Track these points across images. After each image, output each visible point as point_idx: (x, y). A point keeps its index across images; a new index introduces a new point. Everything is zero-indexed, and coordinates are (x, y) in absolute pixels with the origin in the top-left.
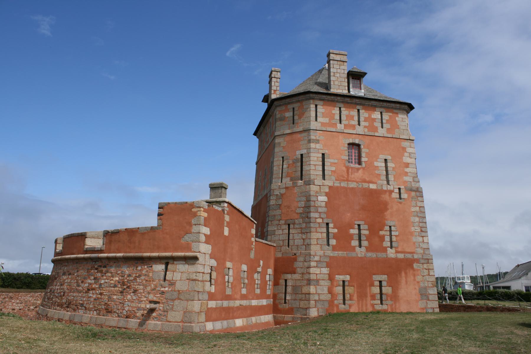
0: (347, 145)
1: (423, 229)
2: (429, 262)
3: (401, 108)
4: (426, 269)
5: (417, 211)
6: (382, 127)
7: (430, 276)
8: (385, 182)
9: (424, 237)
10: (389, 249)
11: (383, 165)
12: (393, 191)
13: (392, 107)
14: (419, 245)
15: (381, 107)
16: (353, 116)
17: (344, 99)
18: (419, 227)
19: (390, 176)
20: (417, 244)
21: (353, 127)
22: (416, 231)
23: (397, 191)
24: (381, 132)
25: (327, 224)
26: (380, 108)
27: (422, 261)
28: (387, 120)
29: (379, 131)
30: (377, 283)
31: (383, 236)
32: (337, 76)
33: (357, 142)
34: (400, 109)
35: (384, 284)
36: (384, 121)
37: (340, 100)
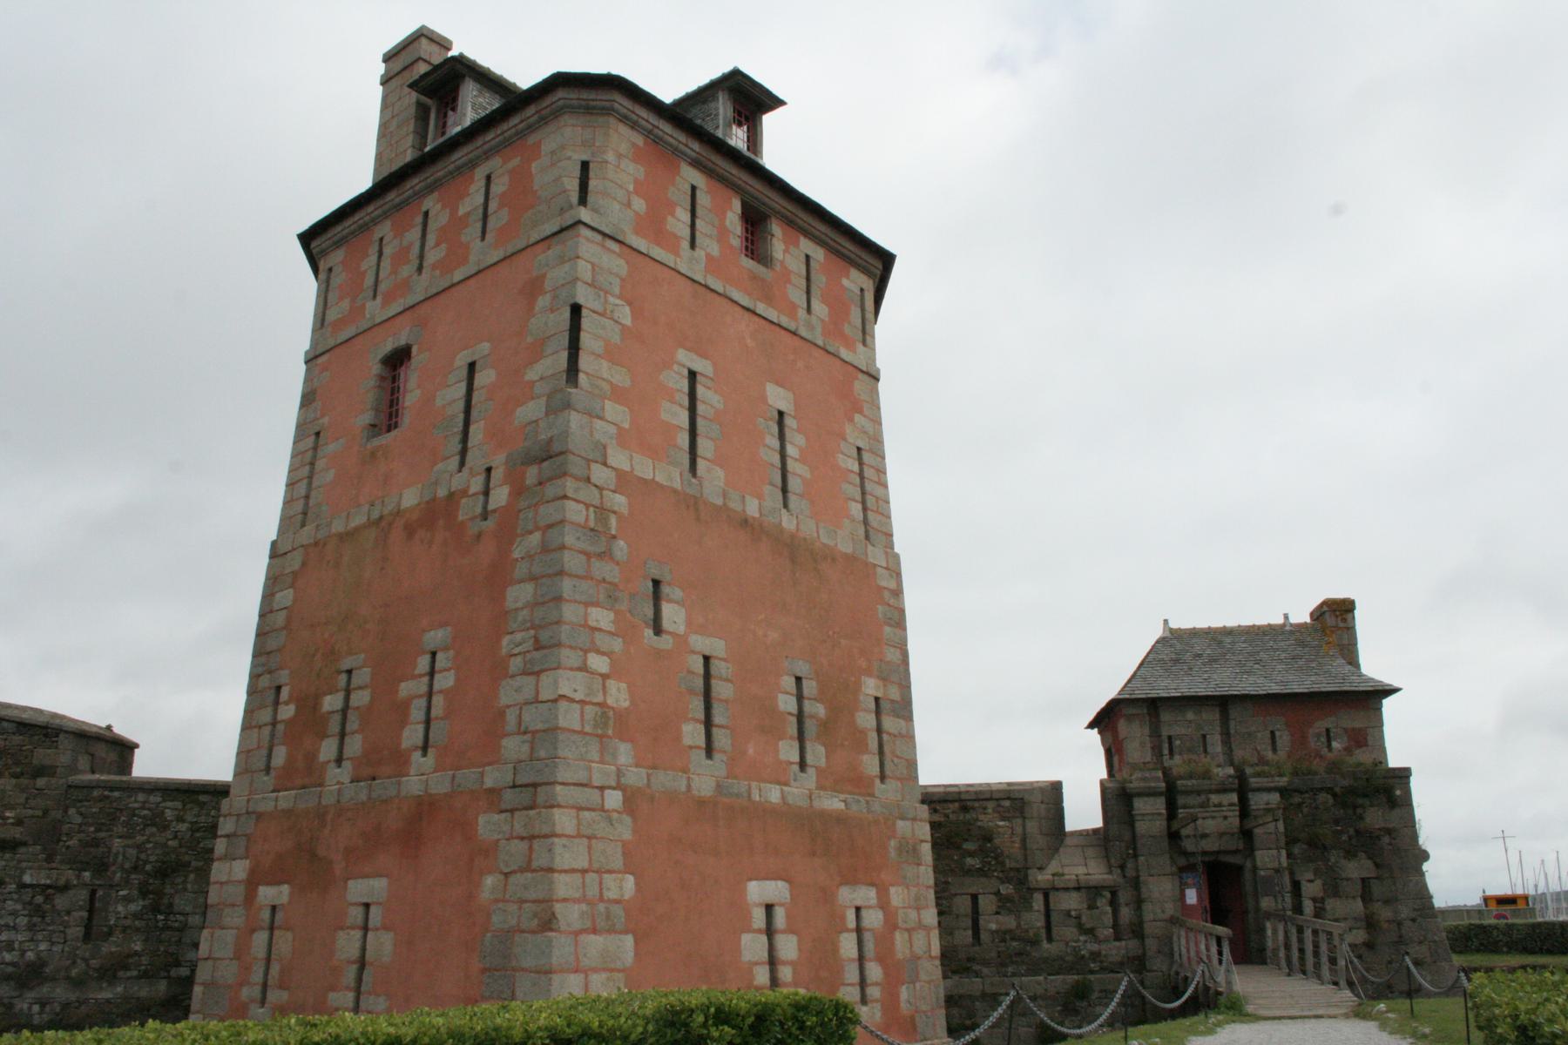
0: (376, 368)
1: (544, 636)
2: (540, 800)
3: (544, 112)
4: (522, 838)
5: (532, 552)
6: (483, 238)
7: (534, 871)
8: (456, 460)
9: (543, 677)
10: (417, 756)
11: (462, 388)
12: (464, 493)
13: (517, 134)
14: (520, 716)
15: (487, 155)
16: (408, 248)
17: (382, 202)
18: (532, 627)
19: (472, 429)
20: (511, 717)
21: (405, 286)
22: (516, 651)
23: (476, 485)
24: (481, 253)
25: (278, 688)
26: (487, 158)
27: (509, 797)
28: (503, 195)
29: (472, 258)
30: (356, 914)
31: (405, 706)
32: (391, 129)
33: (403, 342)
34: (544, 121)
35: (376, 915)
36: (493, 206)
37: (376, 213)
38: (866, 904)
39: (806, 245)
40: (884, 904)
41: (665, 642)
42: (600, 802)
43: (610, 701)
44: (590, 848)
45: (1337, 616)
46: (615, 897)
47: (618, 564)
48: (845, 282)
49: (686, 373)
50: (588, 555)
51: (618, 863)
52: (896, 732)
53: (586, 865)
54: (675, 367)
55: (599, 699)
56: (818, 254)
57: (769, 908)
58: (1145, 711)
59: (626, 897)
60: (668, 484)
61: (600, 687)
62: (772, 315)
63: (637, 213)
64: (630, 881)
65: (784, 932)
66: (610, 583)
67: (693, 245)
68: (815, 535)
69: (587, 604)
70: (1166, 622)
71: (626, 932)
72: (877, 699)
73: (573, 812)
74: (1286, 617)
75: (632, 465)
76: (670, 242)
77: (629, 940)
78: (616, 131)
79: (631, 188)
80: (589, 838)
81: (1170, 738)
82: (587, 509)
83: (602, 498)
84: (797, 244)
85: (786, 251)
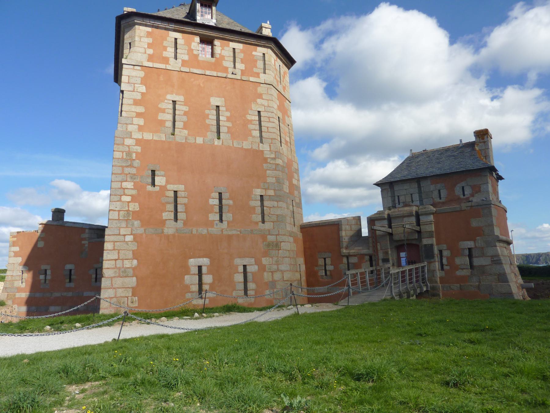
38: (249, 264)
39: (233, 45)
40: (258, 262)
41: (157, 189)
42: (124, 239)
43: (130, 209)
44: (119, 253)
45: (480, 138)
46: (129, 267)
47: (135, 168)
48: (254, 53)
49: (171, 102)
50: (123, 167)
51: (131, 256)
52: (271, 206)
53: (117, 258)
54: (166, 101)
55: (127, 209)
56: (239, 46)
57: (200, 268)
58: (388, 187)
59: (133, 266)
60: (159, 139)
61: (127, 205)
62: (215, 74)
63: (149, 55)
64: (135, 262)
65: (207, 274)
66: (132, 174)
67: (176, 58)
68: (232, 145)
69: (122, 182)
70: (411, 150)
71: (133, 277)
72: (261, 196)
73: (113, 243)
74: (461, 141)
75: (143, 136)
76: (166, 60)
77: (134, 279)
78: (139, 29)
79: (146, 47)
80: (119, 250)
81: (398, 196)
82: (123, 153)
83: (129, 148)
84: (228, 46)
85: (223, 49)
